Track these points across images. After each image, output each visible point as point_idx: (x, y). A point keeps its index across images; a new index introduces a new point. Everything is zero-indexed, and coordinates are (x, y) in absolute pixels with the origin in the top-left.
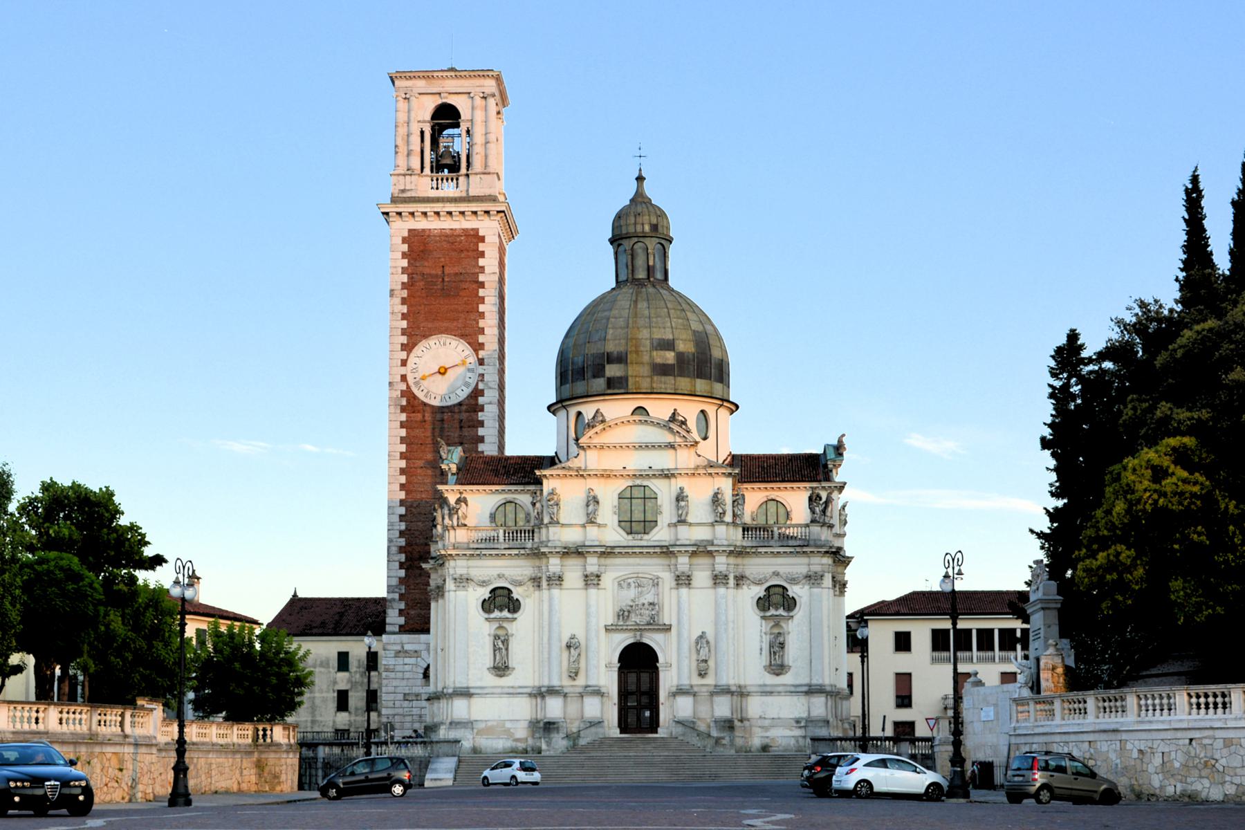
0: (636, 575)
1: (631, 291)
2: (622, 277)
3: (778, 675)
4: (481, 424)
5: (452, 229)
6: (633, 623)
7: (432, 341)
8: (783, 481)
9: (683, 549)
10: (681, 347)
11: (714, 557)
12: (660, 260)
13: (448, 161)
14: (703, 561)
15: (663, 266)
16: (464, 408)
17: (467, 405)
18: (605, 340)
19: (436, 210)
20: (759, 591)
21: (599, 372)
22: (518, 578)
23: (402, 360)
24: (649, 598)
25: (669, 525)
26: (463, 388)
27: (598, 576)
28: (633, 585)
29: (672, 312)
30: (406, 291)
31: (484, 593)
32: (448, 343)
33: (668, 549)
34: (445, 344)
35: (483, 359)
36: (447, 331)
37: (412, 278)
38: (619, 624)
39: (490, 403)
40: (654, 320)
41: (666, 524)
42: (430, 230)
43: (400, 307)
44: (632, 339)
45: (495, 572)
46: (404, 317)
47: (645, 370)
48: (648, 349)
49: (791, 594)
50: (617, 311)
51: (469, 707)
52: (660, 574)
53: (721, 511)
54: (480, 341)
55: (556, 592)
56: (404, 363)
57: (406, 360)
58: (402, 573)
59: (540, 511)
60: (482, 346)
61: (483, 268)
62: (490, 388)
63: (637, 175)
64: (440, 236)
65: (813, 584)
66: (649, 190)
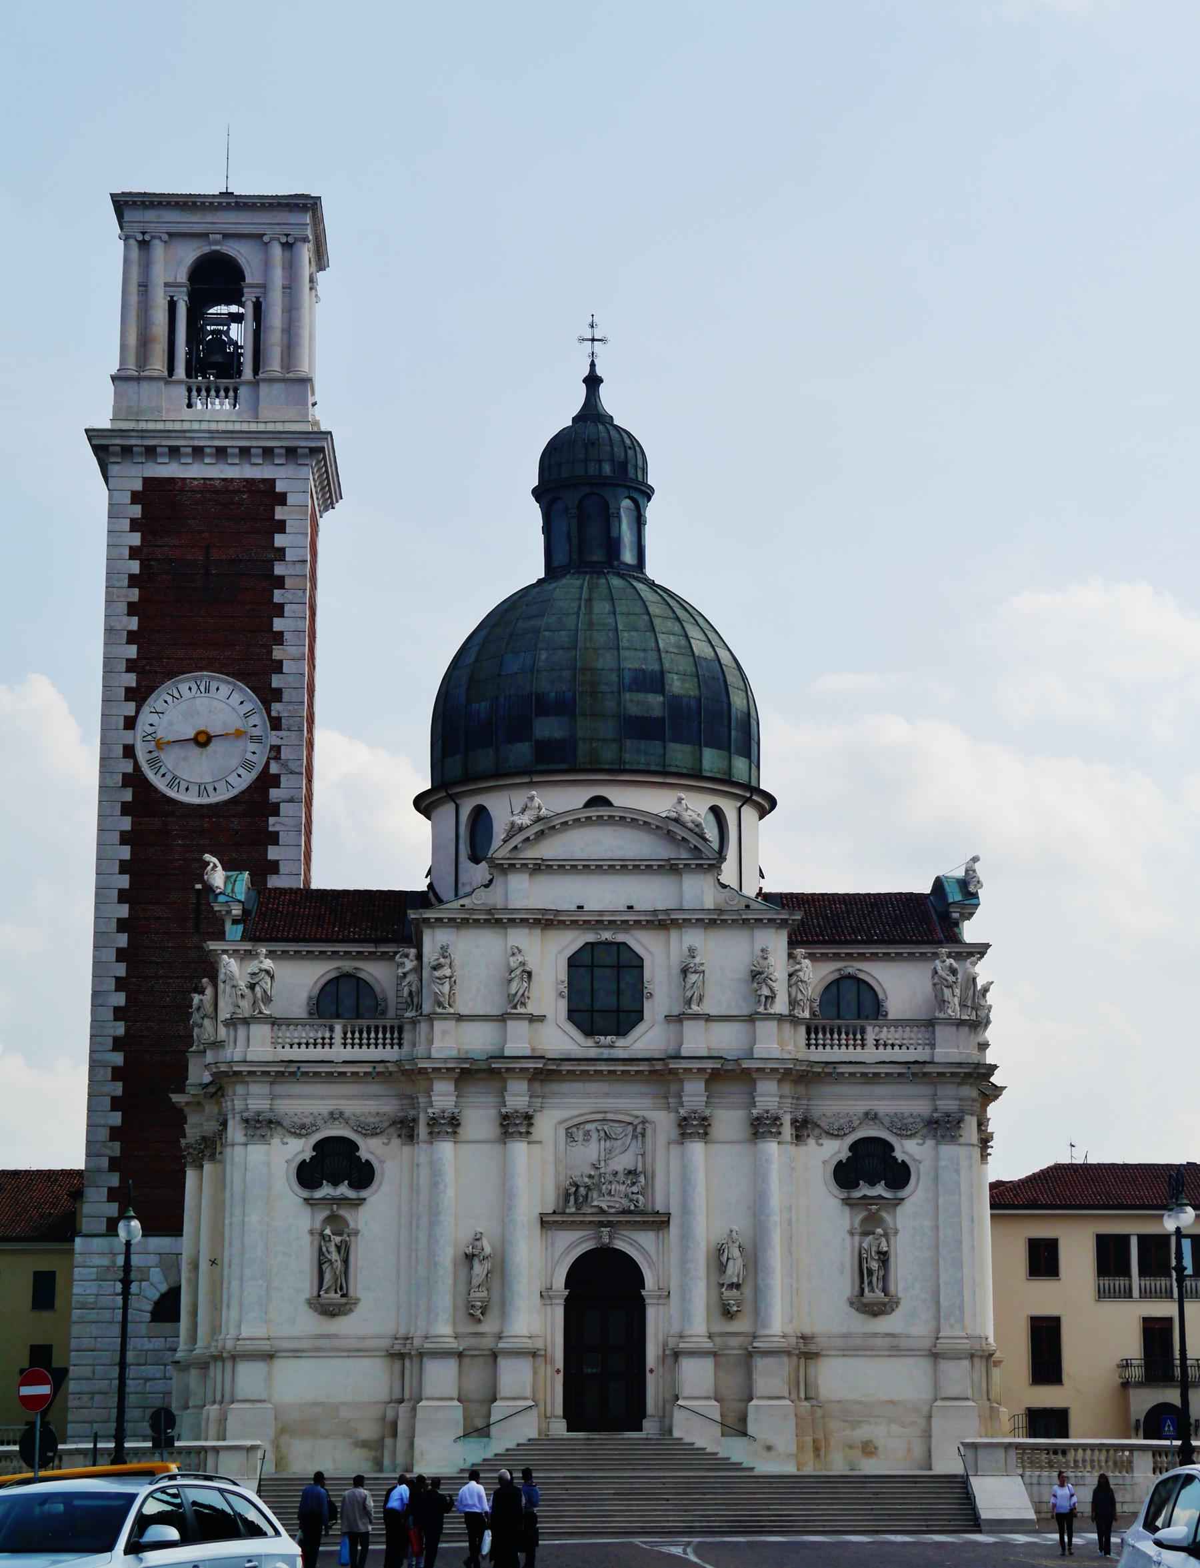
0: (600, 1116)
1: (578, 583)
2: (560, 559)
3: (875, 1315)
4: (274, 839)
5: (224, 480)
6: (594, 1210)
7: (185, 686)
8: (869, 942)
9: (695, 1065)
10: (677, 685)
11: (753, 1082)
12: (630, 528)
13: (218, 358)
14: (733, 1092)
15: (635, 539)
18: (532, 671)
19: (196, 443)
20: (836, 1150)
21: (521, 731)
22: (372, 1120)
23: (126, 718)
24: (623, 1162)
25: (669, 1018)
26: (241, 771)
27: (528, 1118)
28: (595, 1135)
29: (657, 621)
30: (136, 591)
31: (301, 1149)
32: (214, 685)
33: (667, 1065)
34: (207, 690)
35: (279, 719)
38: (568, 1211)
39: (291, 801)
40: (626, 634)
41: (660, 1018)
42: (185, 479)
43: (125, 618)
44: (583, 669)
45: (322, 1107)
46: (132, 637)
47: (607, 729)
48: (615, 689)
49: (899, 1155)
50: (554, 619)
51: (269, 1379)
52: (649, 1115)
53: (766, 991)
54: (274, 685)
55: (446, 1149)
56: (130, 723)
58: (116, 1118)
59: (414, 989)
60: (277, 695)
61: (282, 551)
62: (292, 773)
63: (586, 372)
64: (200, 492)
65: (943, 1137)
66: (609, 400)
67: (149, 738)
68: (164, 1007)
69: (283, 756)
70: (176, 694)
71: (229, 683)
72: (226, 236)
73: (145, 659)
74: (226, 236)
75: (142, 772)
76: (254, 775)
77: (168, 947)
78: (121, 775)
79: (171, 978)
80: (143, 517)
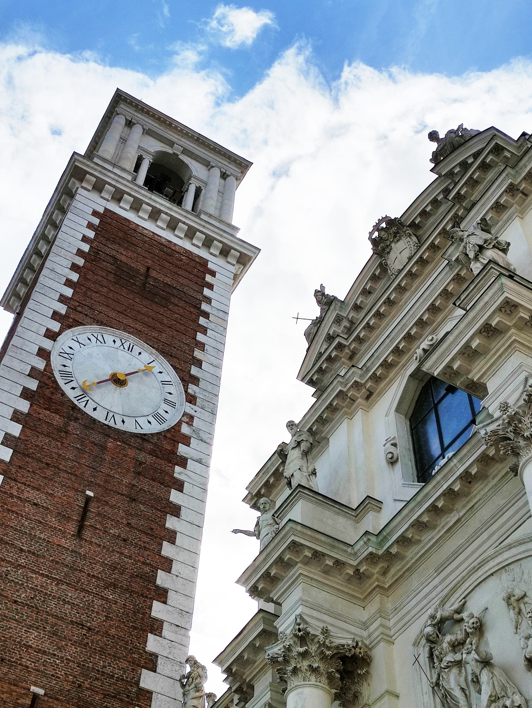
16: (149, 446)
17: (155, 444)
19: (158, 206)
32: (137, 350)
34: (130, 349)
36: (137, 333)
37: (98, 254)
39: (200, 461)
56: (52, 336)
57: (59, 334)
60: (195, 380)
67: (66, 356)
68: (16, 602)
69: (195, 424)
70: (100, 338)
71: (151, 353)
72: (186, 152)
73: (78, 302)
74: (186, 152)
75: (53, 374)
76: (165, 427)
77: (40, 538)
78: (30, 367)
79: (33, 571)
80: (98, 226)
